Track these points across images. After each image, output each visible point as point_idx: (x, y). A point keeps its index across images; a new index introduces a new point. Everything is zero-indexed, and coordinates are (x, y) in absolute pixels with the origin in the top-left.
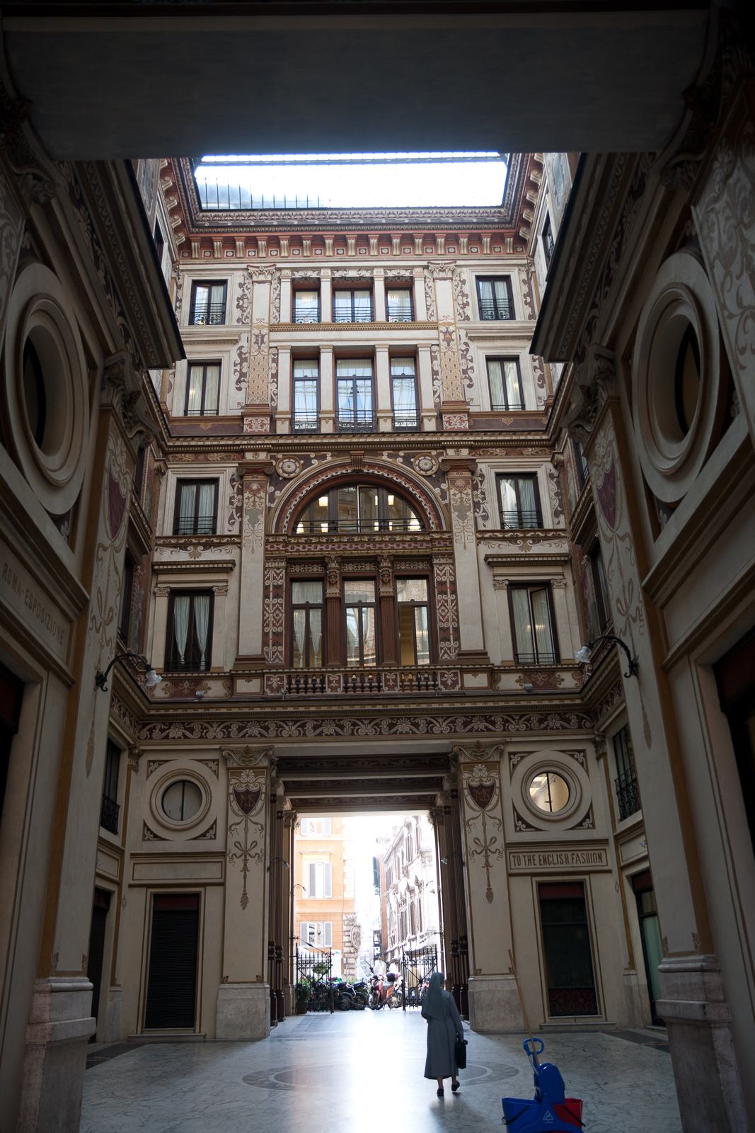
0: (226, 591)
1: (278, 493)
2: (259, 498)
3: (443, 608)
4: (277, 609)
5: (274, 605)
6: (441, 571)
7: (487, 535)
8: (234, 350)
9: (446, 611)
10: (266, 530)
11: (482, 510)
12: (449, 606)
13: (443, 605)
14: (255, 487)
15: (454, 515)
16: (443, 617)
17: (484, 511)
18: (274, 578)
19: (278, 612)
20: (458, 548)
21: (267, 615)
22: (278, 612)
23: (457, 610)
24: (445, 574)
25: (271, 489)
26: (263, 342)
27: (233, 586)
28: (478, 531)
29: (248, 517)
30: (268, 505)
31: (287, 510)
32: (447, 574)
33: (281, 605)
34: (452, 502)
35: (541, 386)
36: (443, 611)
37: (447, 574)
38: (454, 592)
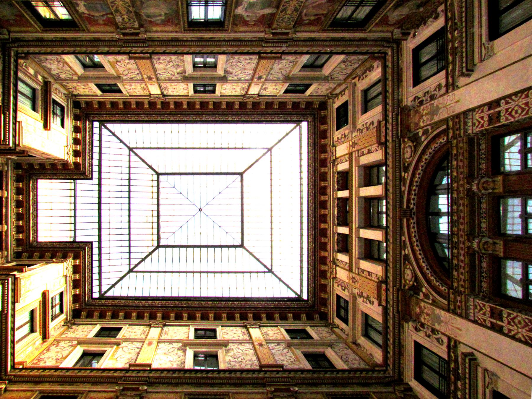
0: (493, 374)
1: (424, 290)
2: (428, 310)
3: (513, 113)
4: (513, 319)
5: (509, 323)
6: (479, 122)
7: (450, 80)
8: (360, 300)
9: (516, 108)
10: (443, 309)
11: (435, 92)
12: (512, 105)
13: (510, 114)
14: (418, 310)
15: (436, 119)
16: (523, 110)
17: (435, 90)
18: (484, 314)
19: (516, 321)
20: (459, 109)
21: (520, 335)
22: (516, 321)
23: (515, 94)
24: (482, 118)
25: (421, 296)
26: (354, 278)
27: (490, 365)
28: (447, 92)
29: (436, 324)
30: (431, 302)
31: (434, 284)
32: (482, 115)
33: (509, 314)
34: (428, 123)
35: (373, 67)
36: (516, 112)
37: (482, 115)
38: (496, 103)
